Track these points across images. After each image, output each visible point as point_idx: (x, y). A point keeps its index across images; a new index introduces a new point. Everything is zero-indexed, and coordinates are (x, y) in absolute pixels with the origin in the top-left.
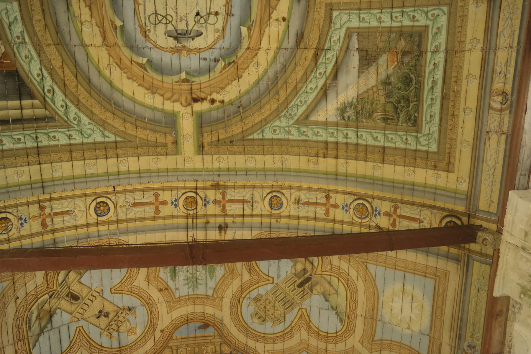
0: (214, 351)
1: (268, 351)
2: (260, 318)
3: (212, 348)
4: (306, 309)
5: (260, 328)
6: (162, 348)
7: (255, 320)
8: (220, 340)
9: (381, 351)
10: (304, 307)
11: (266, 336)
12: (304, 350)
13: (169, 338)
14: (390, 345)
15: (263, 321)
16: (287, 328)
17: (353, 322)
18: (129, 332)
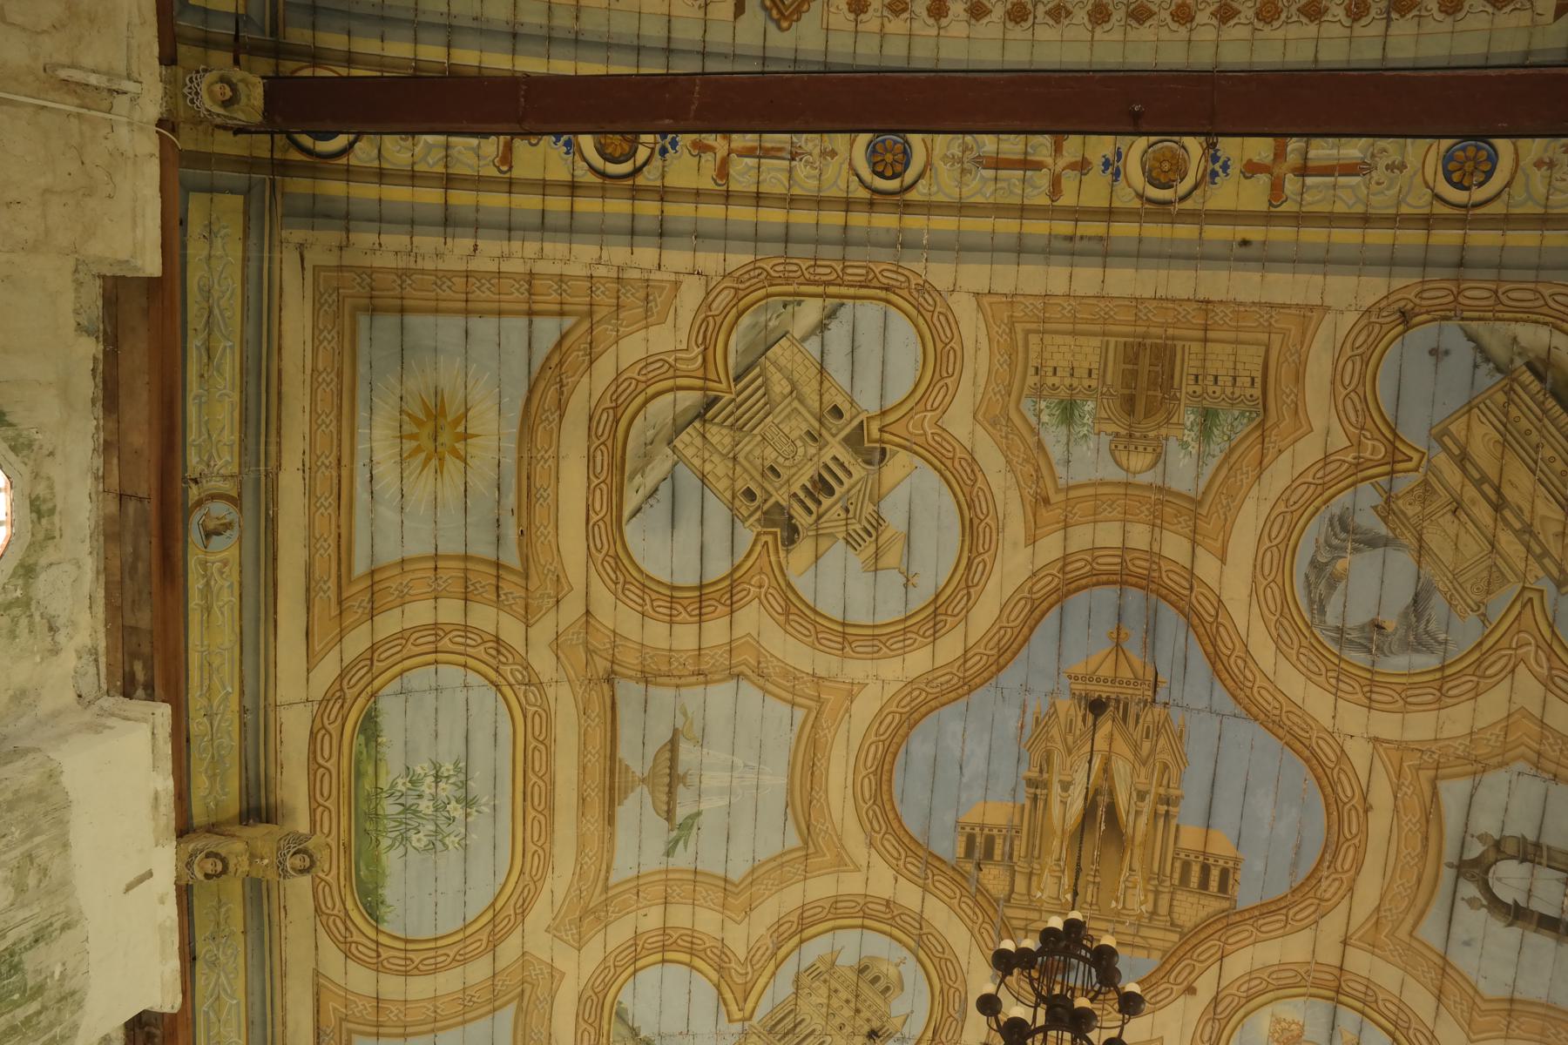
0: (1035, 878)
1: (858, 869)
2: (876, 980)
3: (1039, 888)
4: (730, 1021)
5: (880, 948)
6: (1202, 936)
7: (892, 972)
8: (1010, 912)
9: (494, 975)
10: (737, 1027)
11: (858, 922)
12: (737, 886)
13: (1175, 960)
14: (467, 1009)
15: (867, 967)
16: (792, 951)
17: (585, 1026)
18: (1295, 1033)
